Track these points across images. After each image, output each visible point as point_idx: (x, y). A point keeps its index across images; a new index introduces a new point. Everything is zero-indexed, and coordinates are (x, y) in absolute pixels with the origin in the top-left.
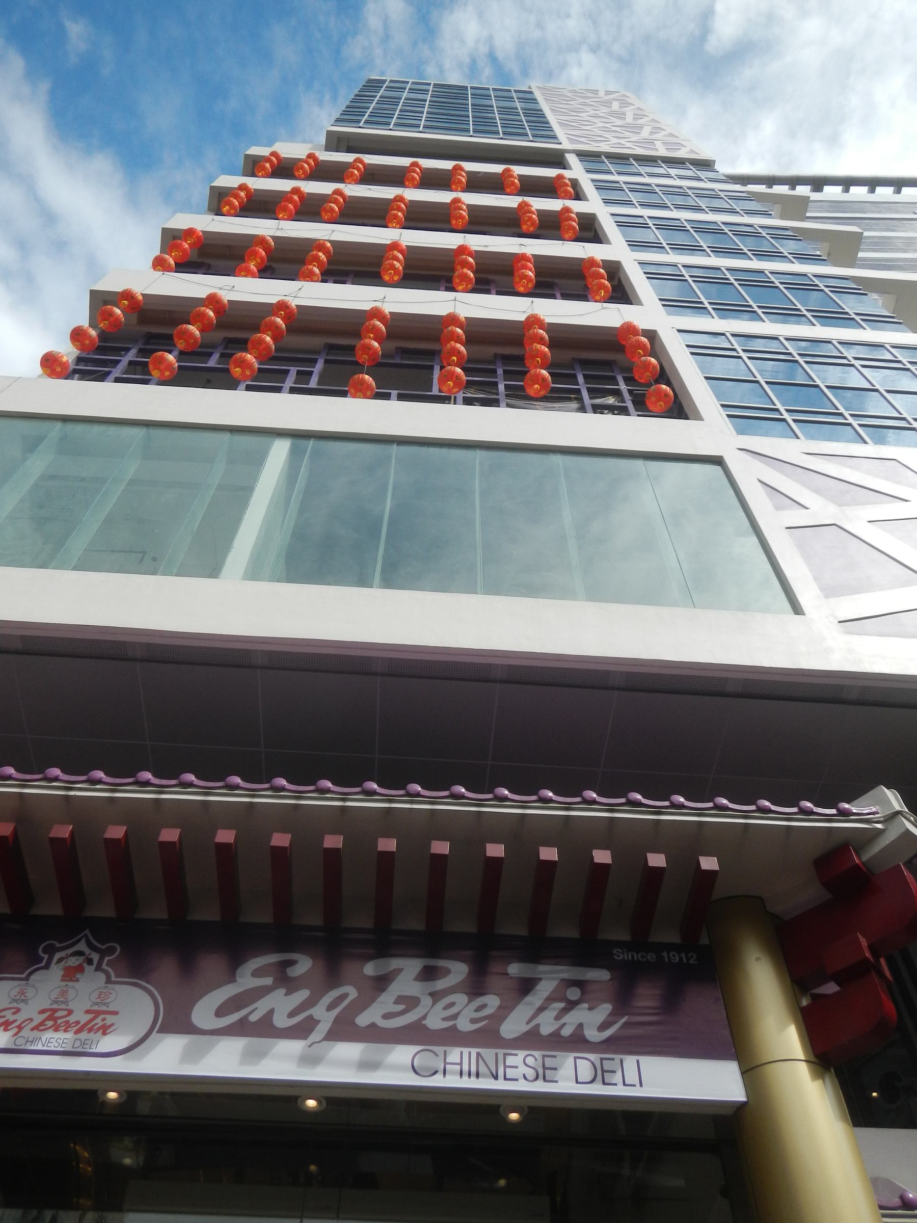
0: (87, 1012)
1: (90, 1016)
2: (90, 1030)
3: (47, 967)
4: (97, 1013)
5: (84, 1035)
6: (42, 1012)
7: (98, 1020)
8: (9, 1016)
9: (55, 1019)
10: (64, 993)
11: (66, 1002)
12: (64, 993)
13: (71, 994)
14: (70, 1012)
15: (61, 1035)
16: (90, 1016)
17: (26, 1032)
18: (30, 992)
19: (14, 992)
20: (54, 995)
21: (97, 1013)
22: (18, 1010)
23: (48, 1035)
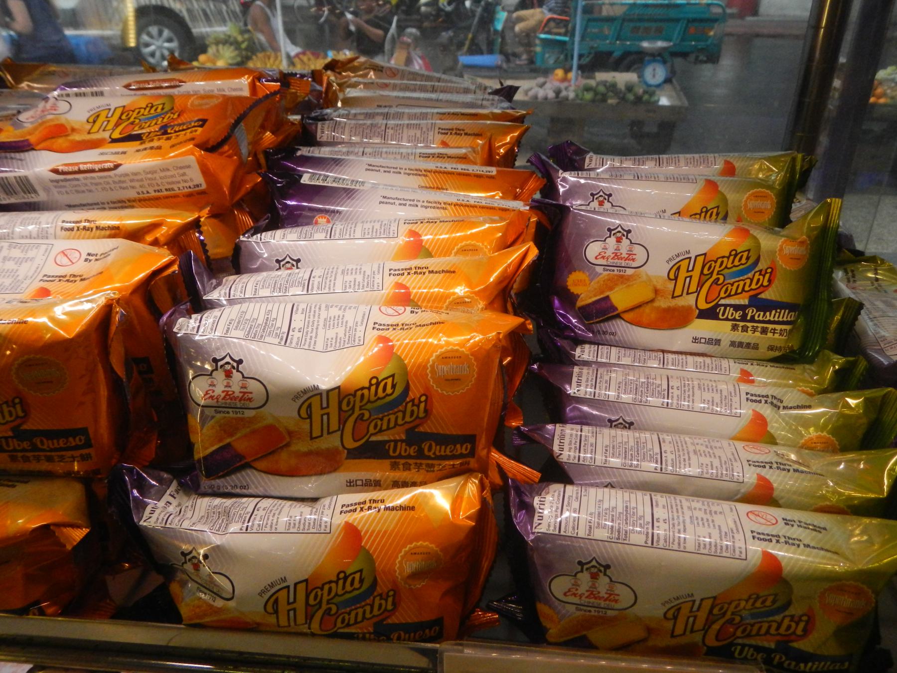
0: (606, 593)
1: (608, 595)
2: (610, 600)
3: (582, 571)
4: (611, 595)
5: (607, 602)
6: (587, 591)
7: (612, 597)
8: (574, 591)
9: (594, 595)
10: (594, 584)
11: (595, 588)
12: (594, 584)
13: (597, 585)
14: (599, 593)
15: (597, 601)
16: (608, 595)
17: (583, 598)
18: (579, 583)
19: (573, 581)
20: (590, 584)
21: (611, 595)
22: (577, 590)
23: (592, 600)
